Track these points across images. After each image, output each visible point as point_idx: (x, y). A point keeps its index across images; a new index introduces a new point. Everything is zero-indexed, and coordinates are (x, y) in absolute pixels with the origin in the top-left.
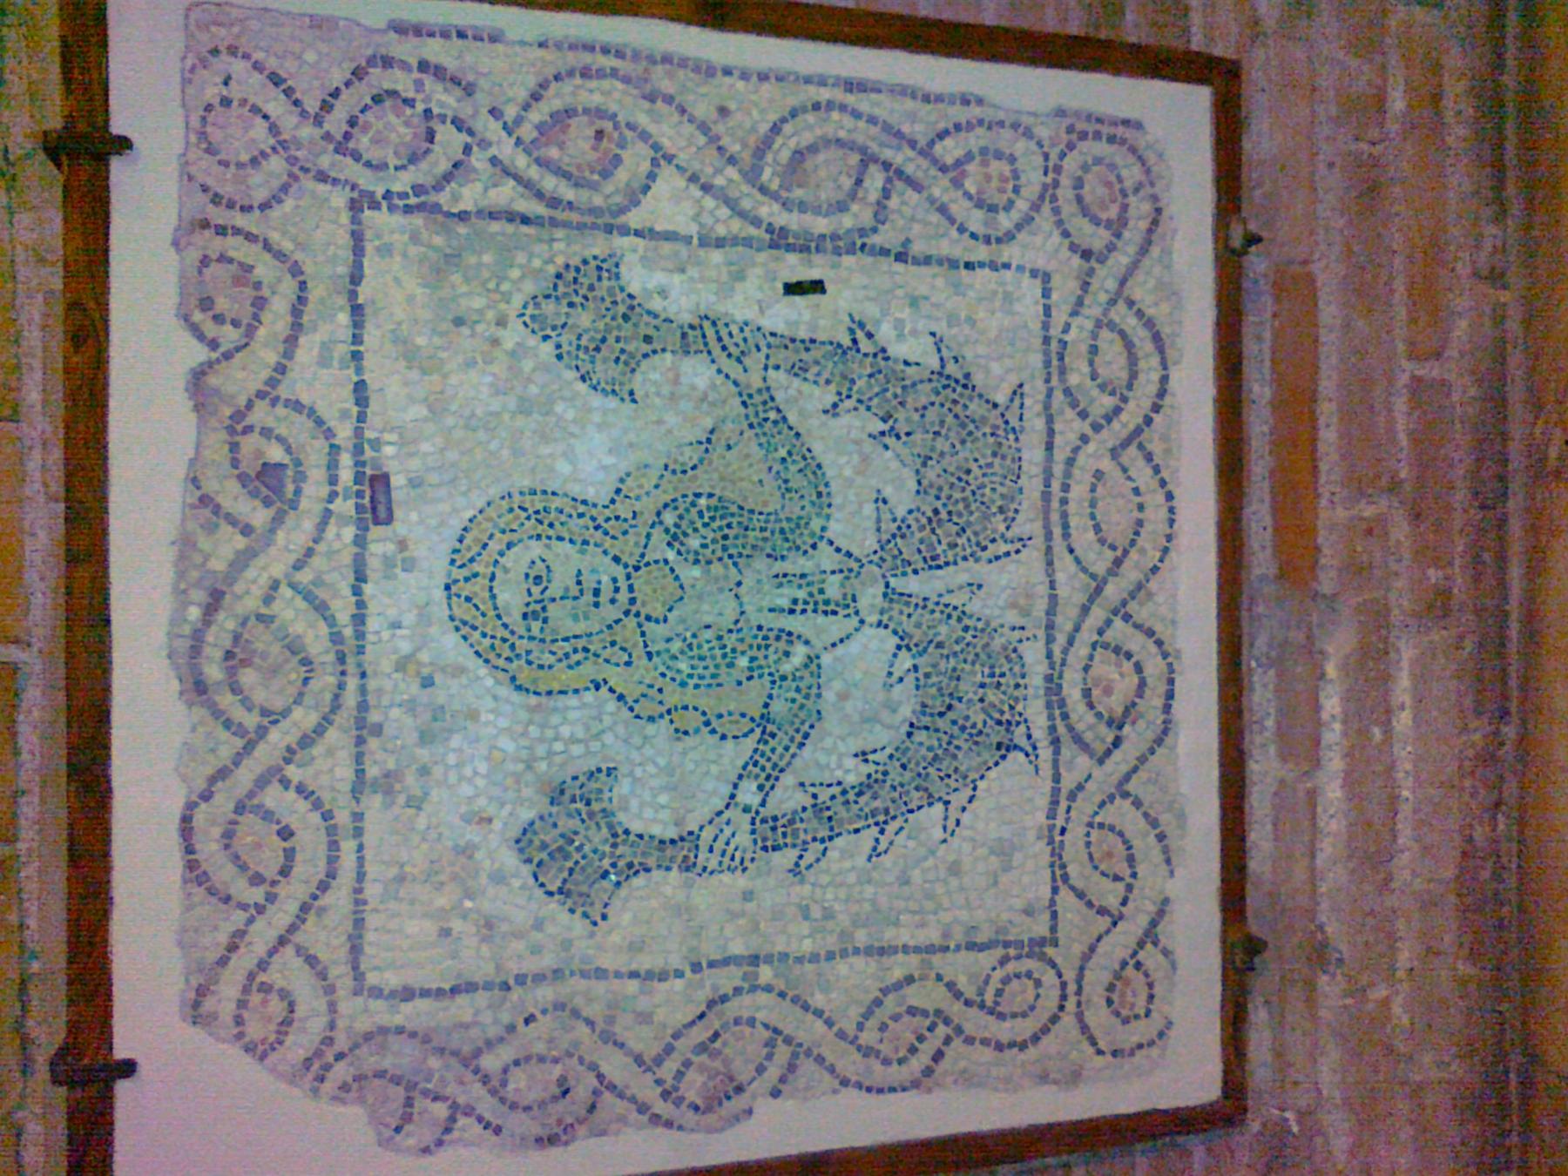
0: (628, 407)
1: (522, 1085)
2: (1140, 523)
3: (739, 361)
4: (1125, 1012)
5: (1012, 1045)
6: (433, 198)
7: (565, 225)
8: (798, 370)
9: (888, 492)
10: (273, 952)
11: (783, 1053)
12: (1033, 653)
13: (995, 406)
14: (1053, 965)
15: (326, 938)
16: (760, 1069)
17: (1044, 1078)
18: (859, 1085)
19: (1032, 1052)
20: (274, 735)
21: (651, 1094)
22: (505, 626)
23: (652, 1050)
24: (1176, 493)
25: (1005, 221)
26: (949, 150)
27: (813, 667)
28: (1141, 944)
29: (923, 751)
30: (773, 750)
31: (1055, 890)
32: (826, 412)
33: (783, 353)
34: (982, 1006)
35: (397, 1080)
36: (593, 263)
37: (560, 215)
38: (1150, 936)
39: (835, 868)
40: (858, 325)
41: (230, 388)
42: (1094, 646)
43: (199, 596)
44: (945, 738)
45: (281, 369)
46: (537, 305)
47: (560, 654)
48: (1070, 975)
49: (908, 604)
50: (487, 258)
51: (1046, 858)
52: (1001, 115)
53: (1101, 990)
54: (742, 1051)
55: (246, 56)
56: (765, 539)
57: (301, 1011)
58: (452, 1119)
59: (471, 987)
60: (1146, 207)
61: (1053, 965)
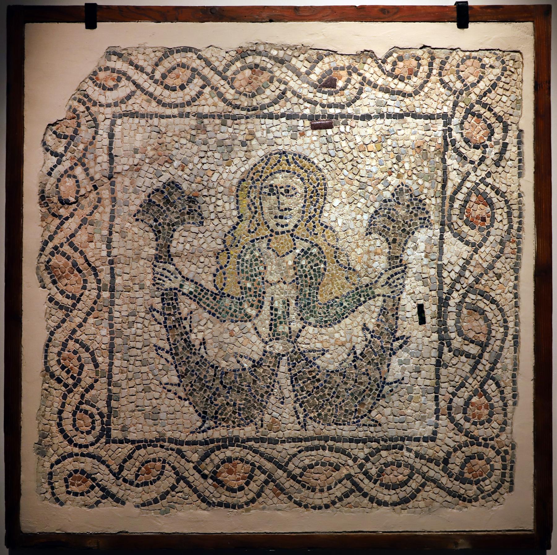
0: (363, 230)
1: (68, 184)
2: (313, 490)
3: (387, 283)
4: (70, 480)
5: (61, 419)
6: (450, 147)
7: (443, 204)
8: (383, 311)
9: (327, 355)
10: (134, 83)
12: (249, 431)
13: (370, 412)
16: (62, 292)
18: (50, 340)
19: (55, 429)
21: (56, 241)
22: (267, 177)
23: (76, 241)
24: (329, 511)
26: (491, 387)
27: (246, 318)
28: (103, 489)
29: (204, 373)
30: (208, 299)
31: (133, 442)
32: (364, 324)
33: (391, 304)
34: (81, 403)
35: (76, 132)
36: (427, 216)
37: (447, 201)
38: (107, 494)
40: (406, 340)
42: (253, 464)
44: (210, 384)
45: (375, 86)
46: (407, 191)
47: (255, 201)
49: (274, 365)
50: (426, 170)
51: (149, 437)
52: (509, 415)
56: (305, 295)
57: (108, 93)
60: (471, 493)
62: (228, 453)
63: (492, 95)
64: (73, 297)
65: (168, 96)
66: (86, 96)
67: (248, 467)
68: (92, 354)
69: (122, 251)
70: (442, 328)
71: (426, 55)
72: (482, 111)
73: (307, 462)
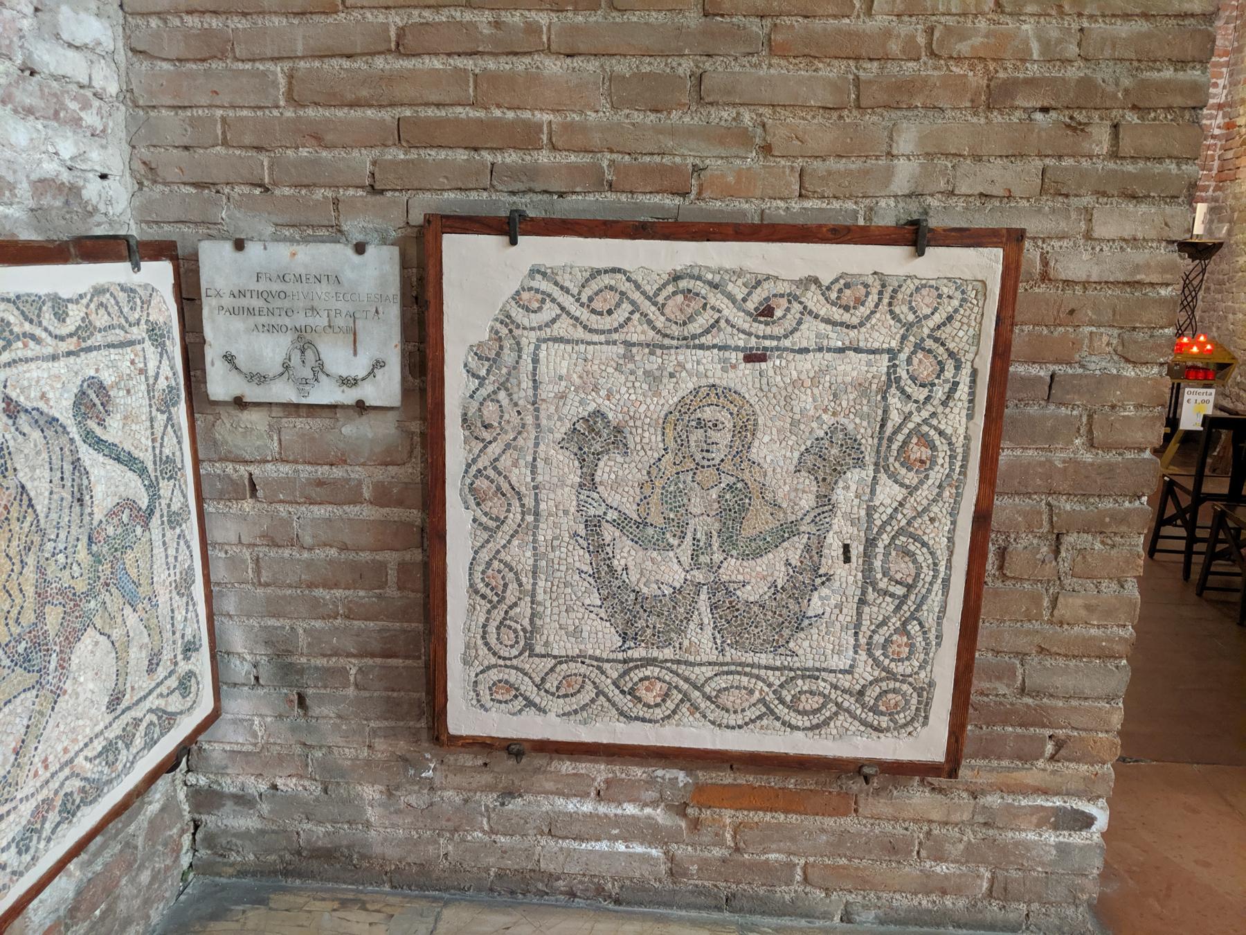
0: (792, 468)
2: (728, 711)
7: (880, 445)
8: (808, 548)
9: (749, 587)
10: (559, 305)
11: (492, 524)
12: (668, 653)
14: (520, 654)
15: (563, 327)
16: (486, 514)
17: (467, 647)
18: (474, 559)
19: (480, 642)
20: (653, 308)
21: (480, 465)
23: (500, 465)
25: (878, 653)
28: (526, 698)
31: (555, 657)
34: (504, 619)
37: (885, 442)
38: (530, 703)
39: (575, 553)
40: (829, 578)
41: (809, 294)
42: (669, 683)
43: (717, 279)
48: (515, 662)
50: (865, 408)
51: (570, 653)
52: (931, 655)
53: (506, 677)
54: (496, 506)
55: (961, 306)
57: (532, 316)
58: (478, 377)
59: (535, 388)
61: (520, 654)
62: (648, 673)
63: (948, 329)
64: (497, 519)
65: (594, 321)
66: (509, 317)
67: (665, 686)
68: (516, 573)
69: (547, 478)
70: (868, 570)
71: (877, 284)
72: (934, 346)
73: (724, 685)
